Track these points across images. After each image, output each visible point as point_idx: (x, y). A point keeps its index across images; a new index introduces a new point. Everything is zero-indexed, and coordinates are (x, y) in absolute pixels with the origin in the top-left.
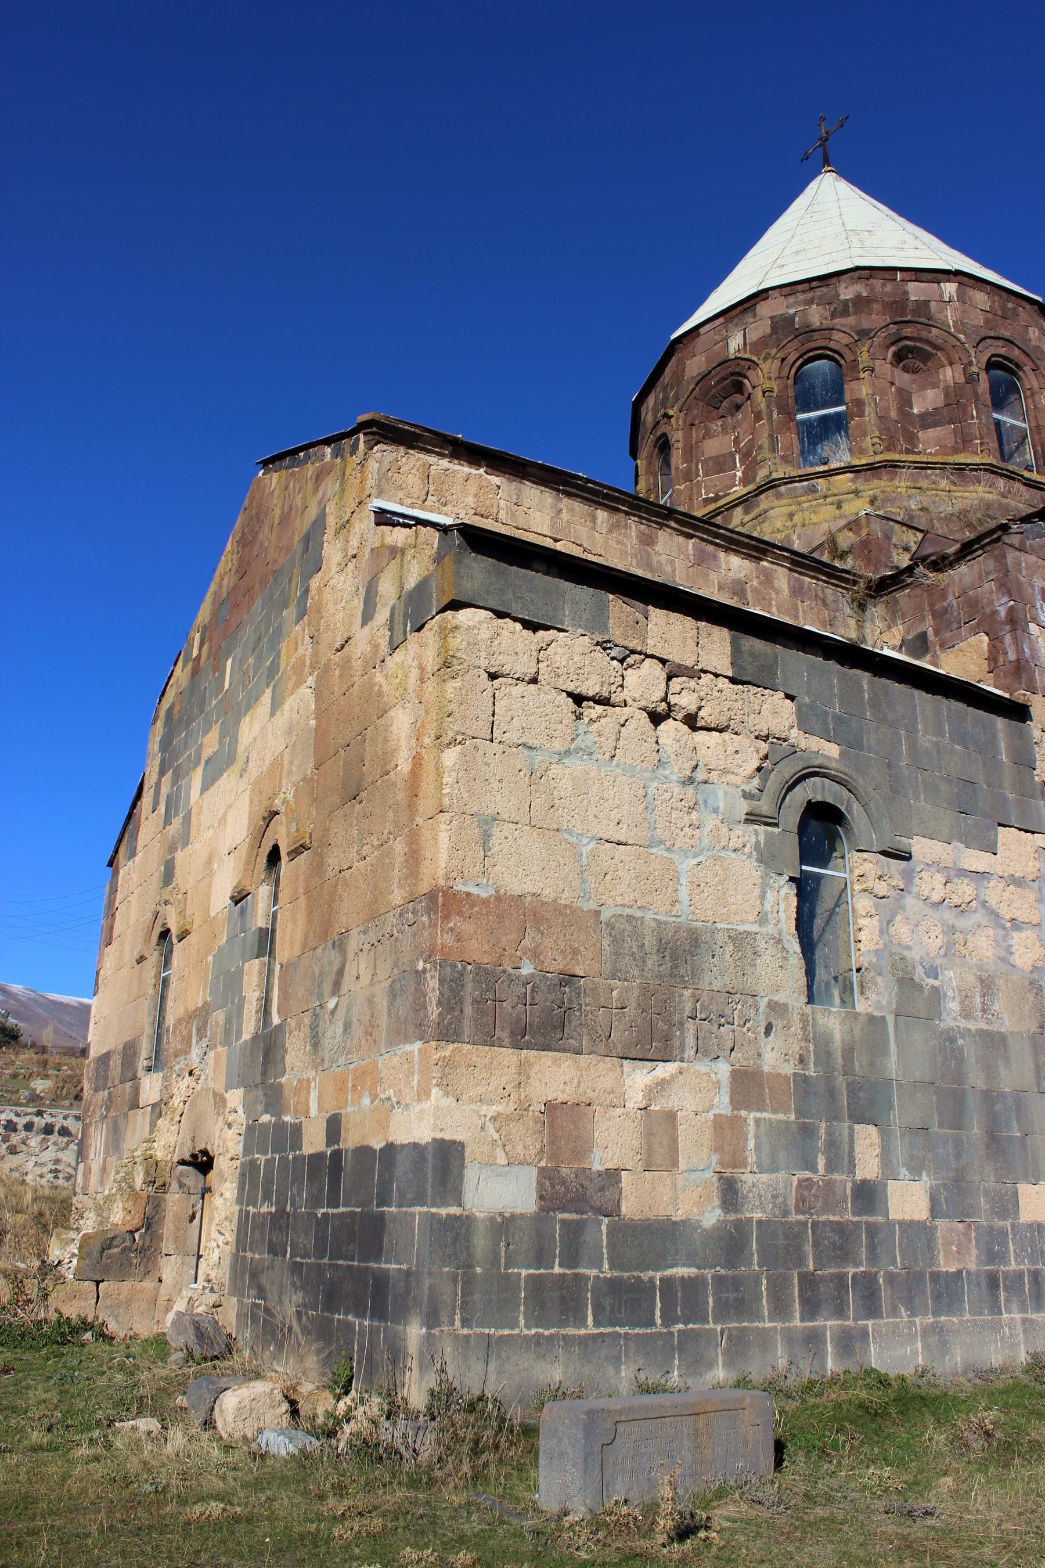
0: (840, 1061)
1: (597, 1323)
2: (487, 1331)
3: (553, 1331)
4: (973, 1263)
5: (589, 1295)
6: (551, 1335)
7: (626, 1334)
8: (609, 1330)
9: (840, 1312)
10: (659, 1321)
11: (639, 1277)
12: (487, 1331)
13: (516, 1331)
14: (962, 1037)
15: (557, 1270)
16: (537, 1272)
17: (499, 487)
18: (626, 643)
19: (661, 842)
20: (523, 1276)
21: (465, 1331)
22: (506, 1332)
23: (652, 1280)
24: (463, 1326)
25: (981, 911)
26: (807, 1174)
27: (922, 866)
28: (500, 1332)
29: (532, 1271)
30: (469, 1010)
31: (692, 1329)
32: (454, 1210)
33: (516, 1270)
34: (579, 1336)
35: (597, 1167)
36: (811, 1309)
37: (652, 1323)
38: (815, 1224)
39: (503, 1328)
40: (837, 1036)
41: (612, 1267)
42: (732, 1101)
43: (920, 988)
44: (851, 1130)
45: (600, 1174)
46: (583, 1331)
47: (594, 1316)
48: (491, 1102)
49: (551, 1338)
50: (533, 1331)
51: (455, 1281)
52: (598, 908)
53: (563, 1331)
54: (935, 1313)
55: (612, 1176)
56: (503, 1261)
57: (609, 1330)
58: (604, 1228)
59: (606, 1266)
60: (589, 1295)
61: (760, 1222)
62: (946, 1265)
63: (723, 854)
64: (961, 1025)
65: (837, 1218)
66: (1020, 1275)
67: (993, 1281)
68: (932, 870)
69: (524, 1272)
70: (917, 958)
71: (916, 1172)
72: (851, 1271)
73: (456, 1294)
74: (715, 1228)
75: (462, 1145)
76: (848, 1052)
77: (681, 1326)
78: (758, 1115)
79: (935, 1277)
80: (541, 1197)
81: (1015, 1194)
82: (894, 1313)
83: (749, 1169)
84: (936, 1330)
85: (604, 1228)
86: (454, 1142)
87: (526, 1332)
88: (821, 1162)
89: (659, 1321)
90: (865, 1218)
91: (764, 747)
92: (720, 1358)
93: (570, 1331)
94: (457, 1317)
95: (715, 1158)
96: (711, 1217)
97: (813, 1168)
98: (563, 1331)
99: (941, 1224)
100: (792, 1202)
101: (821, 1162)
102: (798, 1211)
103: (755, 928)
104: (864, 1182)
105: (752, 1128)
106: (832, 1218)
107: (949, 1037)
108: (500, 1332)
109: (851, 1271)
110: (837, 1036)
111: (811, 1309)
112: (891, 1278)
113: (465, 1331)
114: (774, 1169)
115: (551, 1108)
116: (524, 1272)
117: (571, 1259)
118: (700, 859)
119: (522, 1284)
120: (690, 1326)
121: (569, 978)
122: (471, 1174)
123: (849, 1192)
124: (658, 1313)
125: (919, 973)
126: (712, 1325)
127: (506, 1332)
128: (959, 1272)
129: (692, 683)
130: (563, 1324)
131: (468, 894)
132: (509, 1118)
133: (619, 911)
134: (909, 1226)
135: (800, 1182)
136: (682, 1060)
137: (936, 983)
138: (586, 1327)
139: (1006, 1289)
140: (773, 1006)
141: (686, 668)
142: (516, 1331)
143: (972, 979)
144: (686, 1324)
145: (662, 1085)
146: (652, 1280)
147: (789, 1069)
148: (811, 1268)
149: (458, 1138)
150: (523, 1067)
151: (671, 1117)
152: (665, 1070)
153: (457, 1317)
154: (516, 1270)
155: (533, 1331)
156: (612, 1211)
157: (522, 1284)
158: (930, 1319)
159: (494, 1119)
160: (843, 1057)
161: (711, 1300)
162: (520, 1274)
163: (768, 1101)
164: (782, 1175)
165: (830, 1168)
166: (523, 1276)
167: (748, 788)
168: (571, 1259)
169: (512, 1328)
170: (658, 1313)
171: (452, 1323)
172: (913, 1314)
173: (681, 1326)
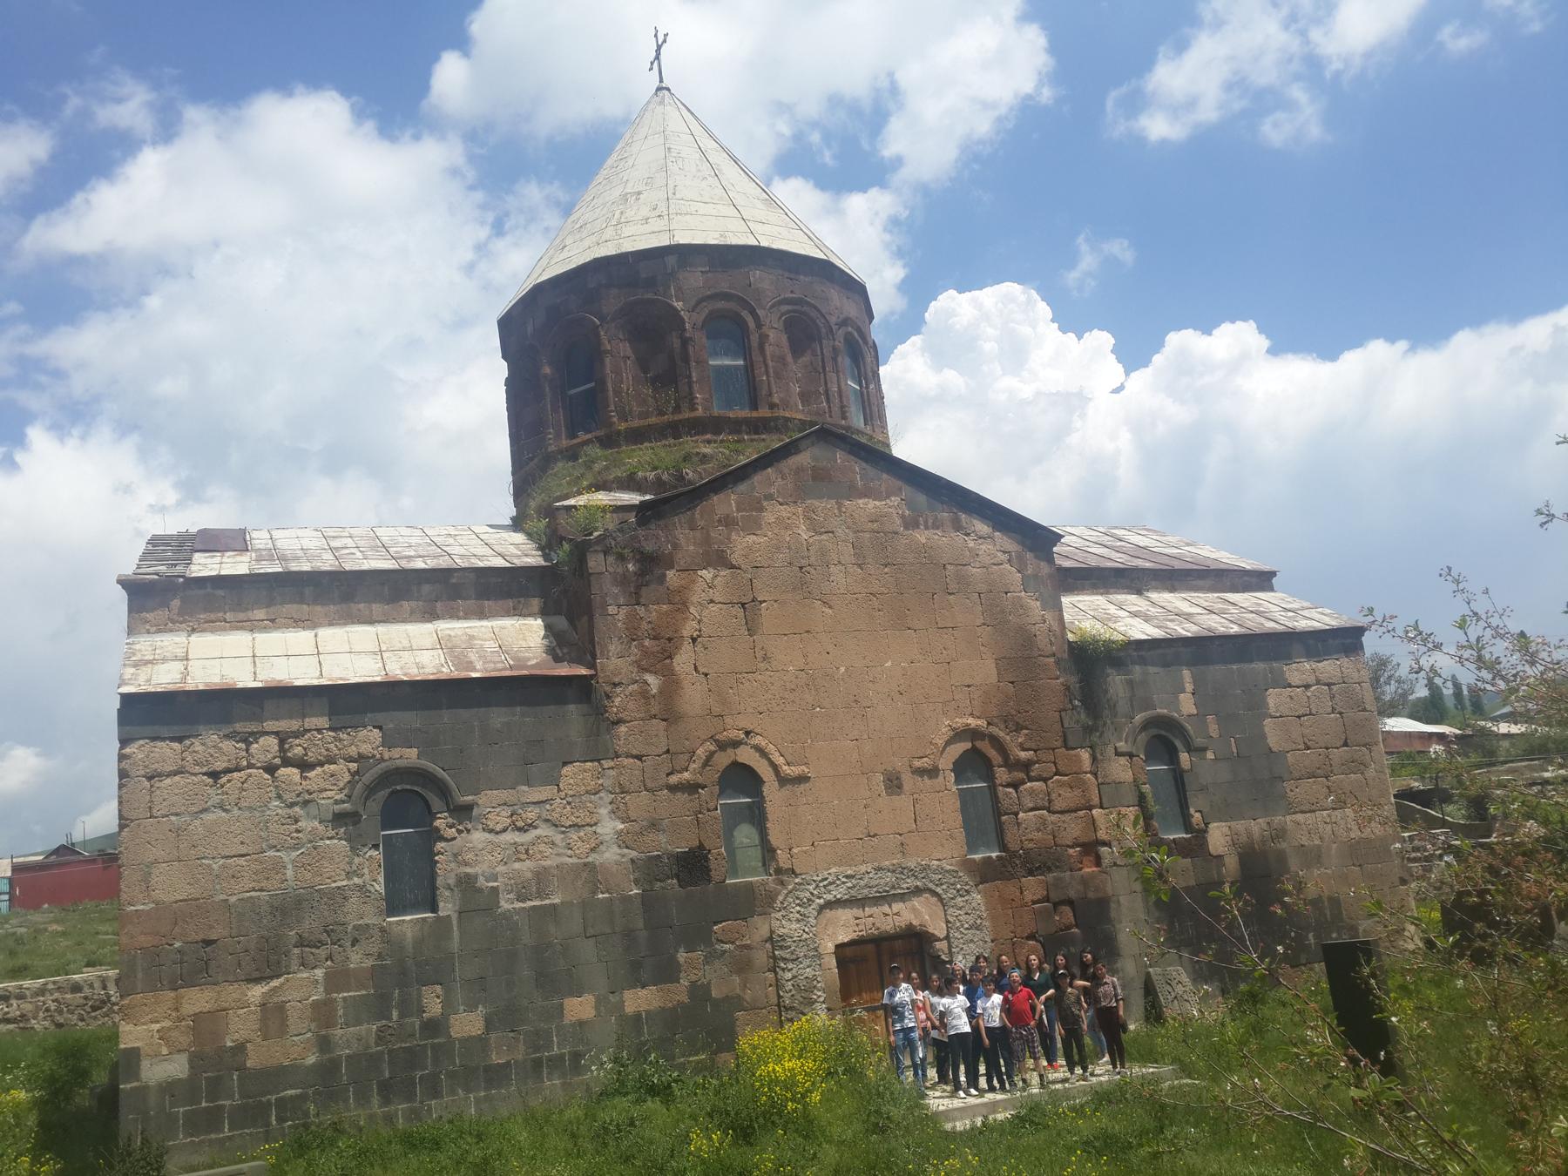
0: (411, 950)
3: (202, 1137)
4: (520, 1054)
5: (226, 1115)
9: (410, 1097)
10: (274, 1123)
11: (260, 1100)
14: (518, 914)
15: (204, 1104)
16: (190, 1108)
17: (224, 597)
18: (245, 730)
19: (275, 847)
23: (269, 1100)
25: (543, 825)
26: (384, 1022)
27: (489, 809)
30: (140, 975)
32: (135, 1084)
35: (229, 1044)
36: (386, 1101)
38: (390, 1052)
40: (409, 934)
41: (242, 1097)
42: (325, 989)
43: (480, 890)
44: (419, 990)
45: (231, 1048)
46: (221, 1135)
48: (158, 1022)
49: (202, 1142)
52: (227, 898)
53: (209, 1137)
54: (486, 1089)
55: (240, 1048)
56: (167, 1107)
58: (235, 1077)
59: (237, 1096)
61: (348, 1056)
62: (496, 1059)
63: (321, 843)
64: (517, 906)
65: (408, 1045)
66: (562, 1057)
67: (538, 1064)
68: (498, 810)
69: (181, 1110)
70: (480, 872)
71: (471, 1007)
72: (419, 1074)
74: (313, 1065)
75: (138, 1048)
76: (419, 942)
77: (290, 1123)
78: (345, 994)
79: (488, 1069)
80: (191, 1067)
81: (562, 1004)
82: (453, 1092)
83: (339, 1026)
84: (488, 1098)
85: (235, 1077)
86: (133, 1048)
88: (395, 1015)
90: (430, 1041)
91: (353, 766)
93: (213, 1136)
95: (313, 1026)
96: (311, 1060)
97: (389, 1019)
98: (209, 1137)
99: (493, 1036)
100: (372, 1041)
101: (395, 1015)
102: (377, 1045)
103: (344, 883)
104: (430, 1020)
105: (341, 1004)
106: (403, 1045)
107: (507, 916)
109: (419, 1074)
110: (409, 934)
111: (386, 1101)
112: (452, 1075)
114: (358, 1023)
115: (196, 1017)
116: (181, 1110)
117: (213, 1095)
118: (302, 850)
119: (181, 1116)
121: (208, 943)
122: (145, 1064)
123: (417, 1027)
125: (481, 882)
128: (508, 1063)
129: (297, 741)
130: (211, 1132)
131: (136, 910)
132: (169, 1029)
133: (241, 896)
134: (466, 1041)
135: (379, 1030)
136: (288, 974)
137: (495, 884)
138: (224, 1132)
139: (548, 1066)
140: (356, 928)
141: (292, 732)
143: (529, 875)
145: (274, 989)
146: (269, 1100)
147: (369, 963)
148: (387, 1075)
149: (136, 1045)
150: (178, 1000)
151: (281, 1008)
152: (275, 983)
155: (189, 1140)
156: (241, 1068)
157: (181, 1116)
158: (483, 1094)
159: (158, 1031)
160: (414, 948)
163: (353, 985)
164: (365, 1027)
165: (402, 1016)
167: (337, 797)
168: (213, 1095)
172: (468, 1090)
173: (290, 1123)
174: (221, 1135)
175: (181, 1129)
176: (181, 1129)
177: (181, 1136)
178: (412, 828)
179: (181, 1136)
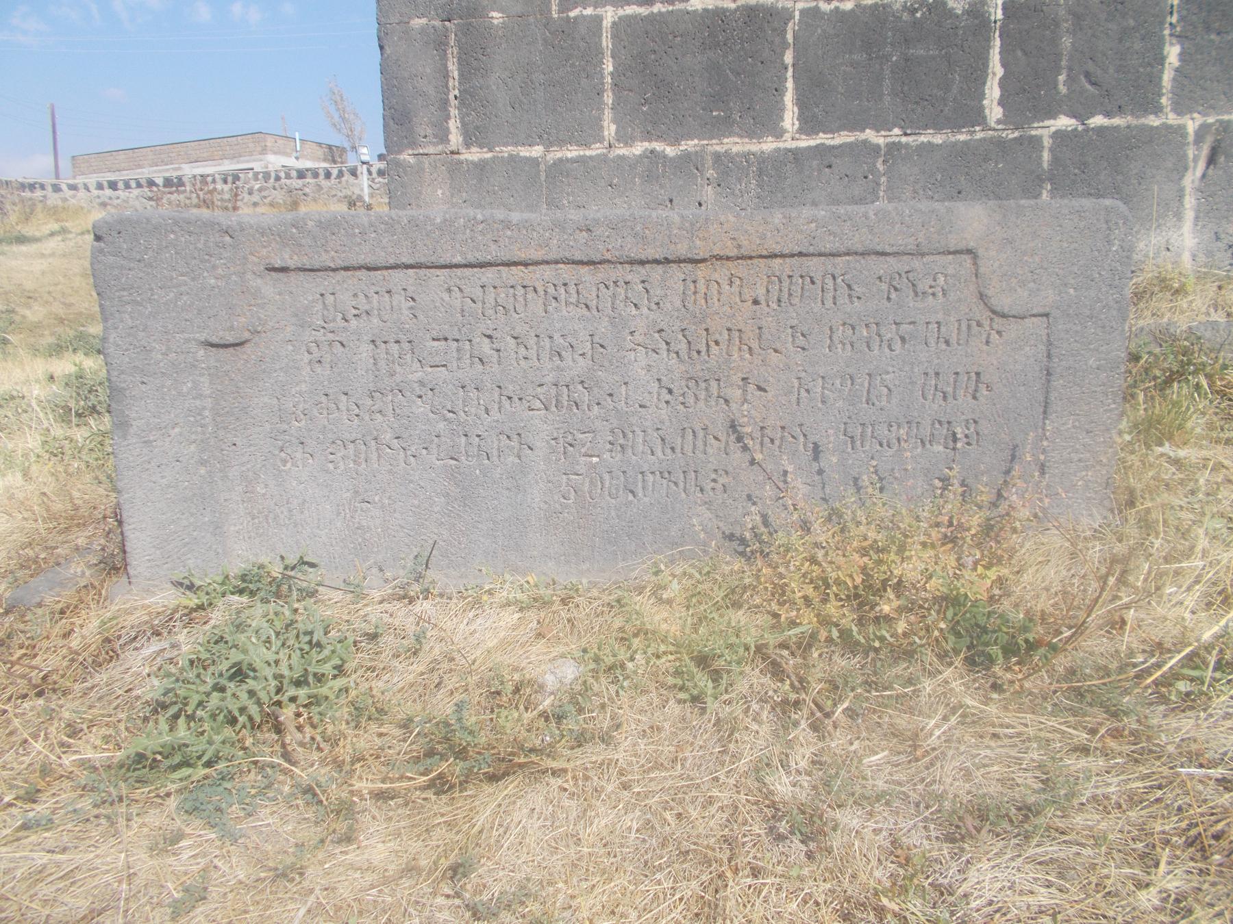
1: (809, 125)
2: (525, 152)
3: (690, 145)
5: (788, 58)
6: (686, 157)
7: (893, 147)
8: (844, 138)
10: (994, 112)
12: (525, 152)
13: (596, 150)
16: (643, 11)
20: (607, 23)
21: (474, 155)
22: (572, 152)
24: (468, 145)
28: (557, 154)
29: (631, 10)
31: (1100, 130)
33: (589, 11)
34: (762, 159)
37: (978, 117)
39: (561, 143)
46: (769, 145)
47: (801, 102)
49: (689, 163)
50: (639, 148)
51: (441, 44)
53: (716, 146)
57: (844, 138)
60: (788, 58)
69: (609, 15)
73: (446, 75)
77: (1064, 122)
87: (622, 151)
89: (994, 112)
92: (1189, 202)
93: (735, 145)
94: (453, 125)
98: (716, 146)
108: (557, 154)
113: (474, 155)
116: (609, 15)
119: (606, 42)
120: (1098, 121)
124: (993, 91)
126: (1172, 119)
127: (572, 152)
130: (723, 127)
138: (779, 134)
142: (596, 150)
144: (1081, 118)
153: (453, 125)
154: (589, 11)
155: (639, 148)
157: (606, 42)
161: (1173, 53)
162: (598, 20)
166: (607, 23)
169: (587, 145)
170: (993, 91)
171: (444, 138)
173: (1064, 122)
174: (769, 145)
175: (608, 98)
176: (608, 98)
177: (610, 129)
178: (987, 48)
179: (610, 129)
